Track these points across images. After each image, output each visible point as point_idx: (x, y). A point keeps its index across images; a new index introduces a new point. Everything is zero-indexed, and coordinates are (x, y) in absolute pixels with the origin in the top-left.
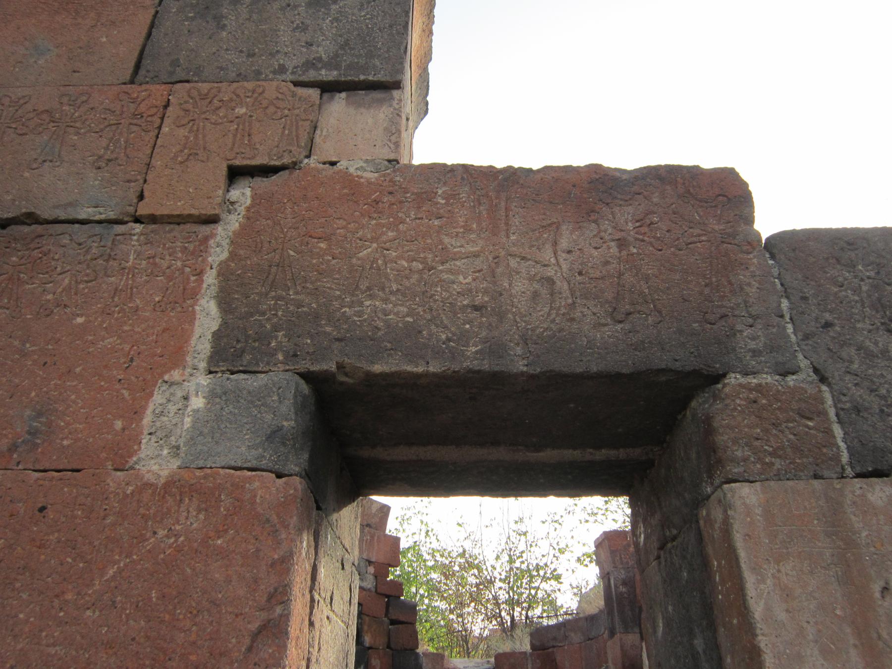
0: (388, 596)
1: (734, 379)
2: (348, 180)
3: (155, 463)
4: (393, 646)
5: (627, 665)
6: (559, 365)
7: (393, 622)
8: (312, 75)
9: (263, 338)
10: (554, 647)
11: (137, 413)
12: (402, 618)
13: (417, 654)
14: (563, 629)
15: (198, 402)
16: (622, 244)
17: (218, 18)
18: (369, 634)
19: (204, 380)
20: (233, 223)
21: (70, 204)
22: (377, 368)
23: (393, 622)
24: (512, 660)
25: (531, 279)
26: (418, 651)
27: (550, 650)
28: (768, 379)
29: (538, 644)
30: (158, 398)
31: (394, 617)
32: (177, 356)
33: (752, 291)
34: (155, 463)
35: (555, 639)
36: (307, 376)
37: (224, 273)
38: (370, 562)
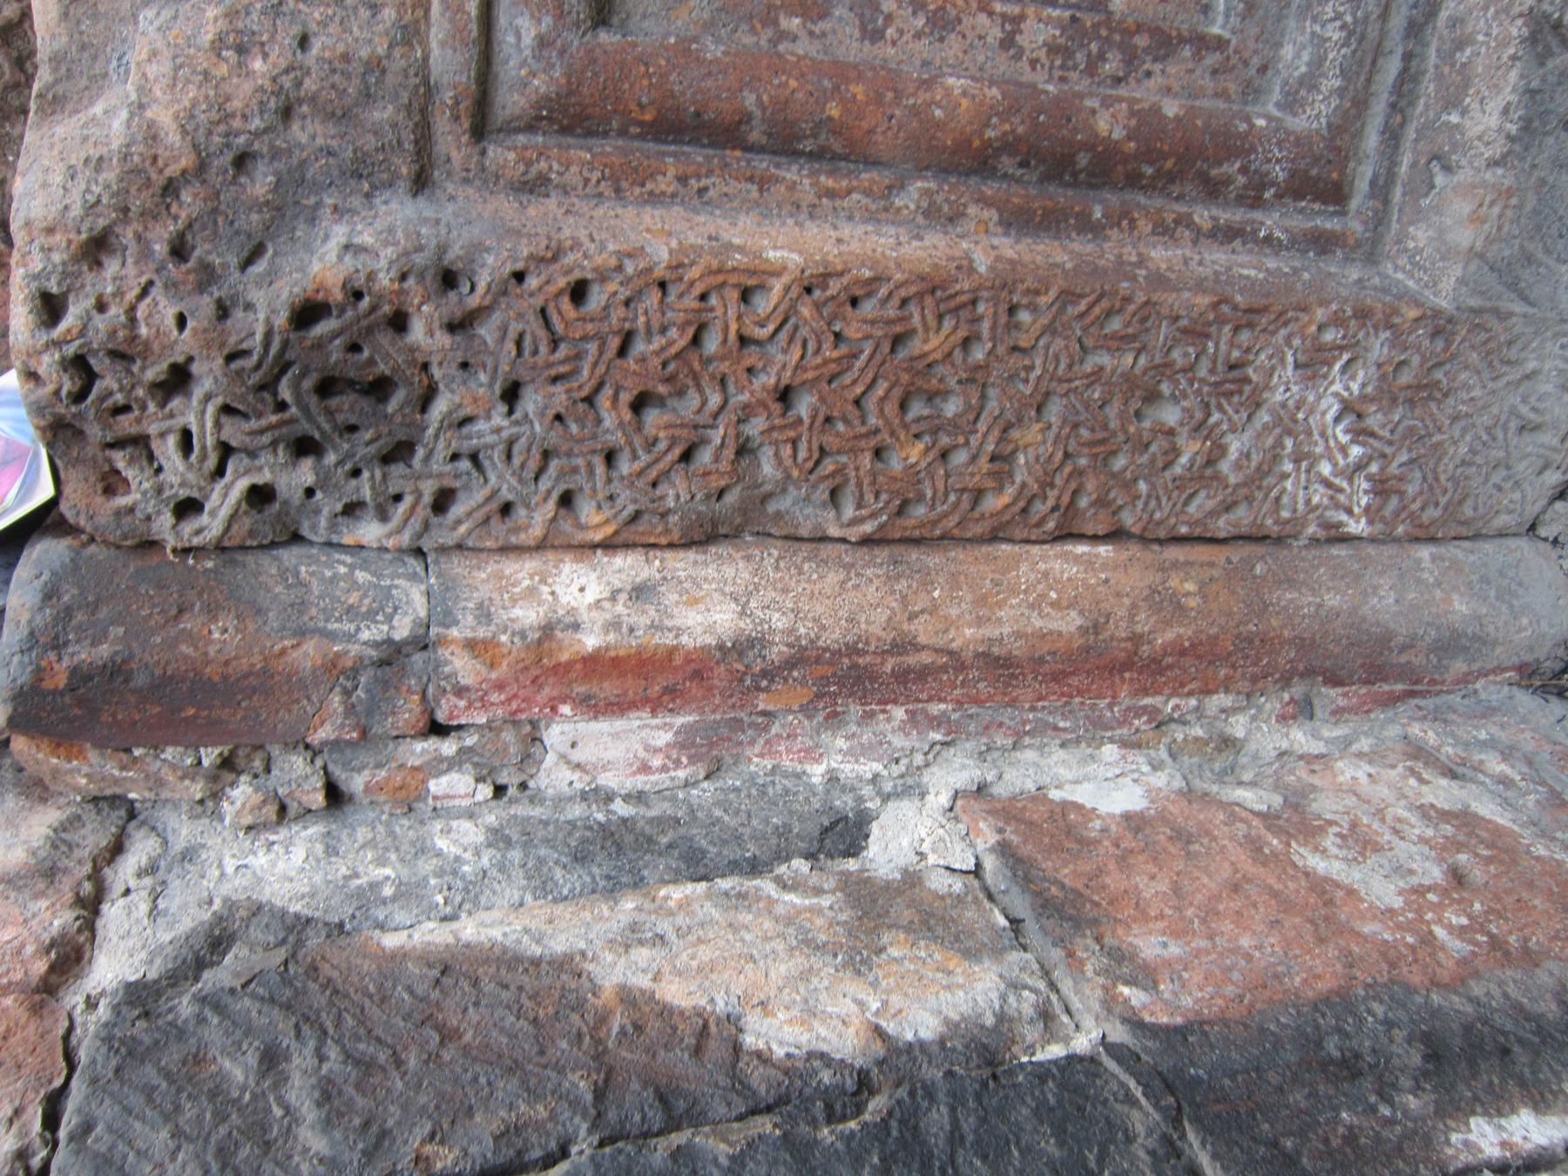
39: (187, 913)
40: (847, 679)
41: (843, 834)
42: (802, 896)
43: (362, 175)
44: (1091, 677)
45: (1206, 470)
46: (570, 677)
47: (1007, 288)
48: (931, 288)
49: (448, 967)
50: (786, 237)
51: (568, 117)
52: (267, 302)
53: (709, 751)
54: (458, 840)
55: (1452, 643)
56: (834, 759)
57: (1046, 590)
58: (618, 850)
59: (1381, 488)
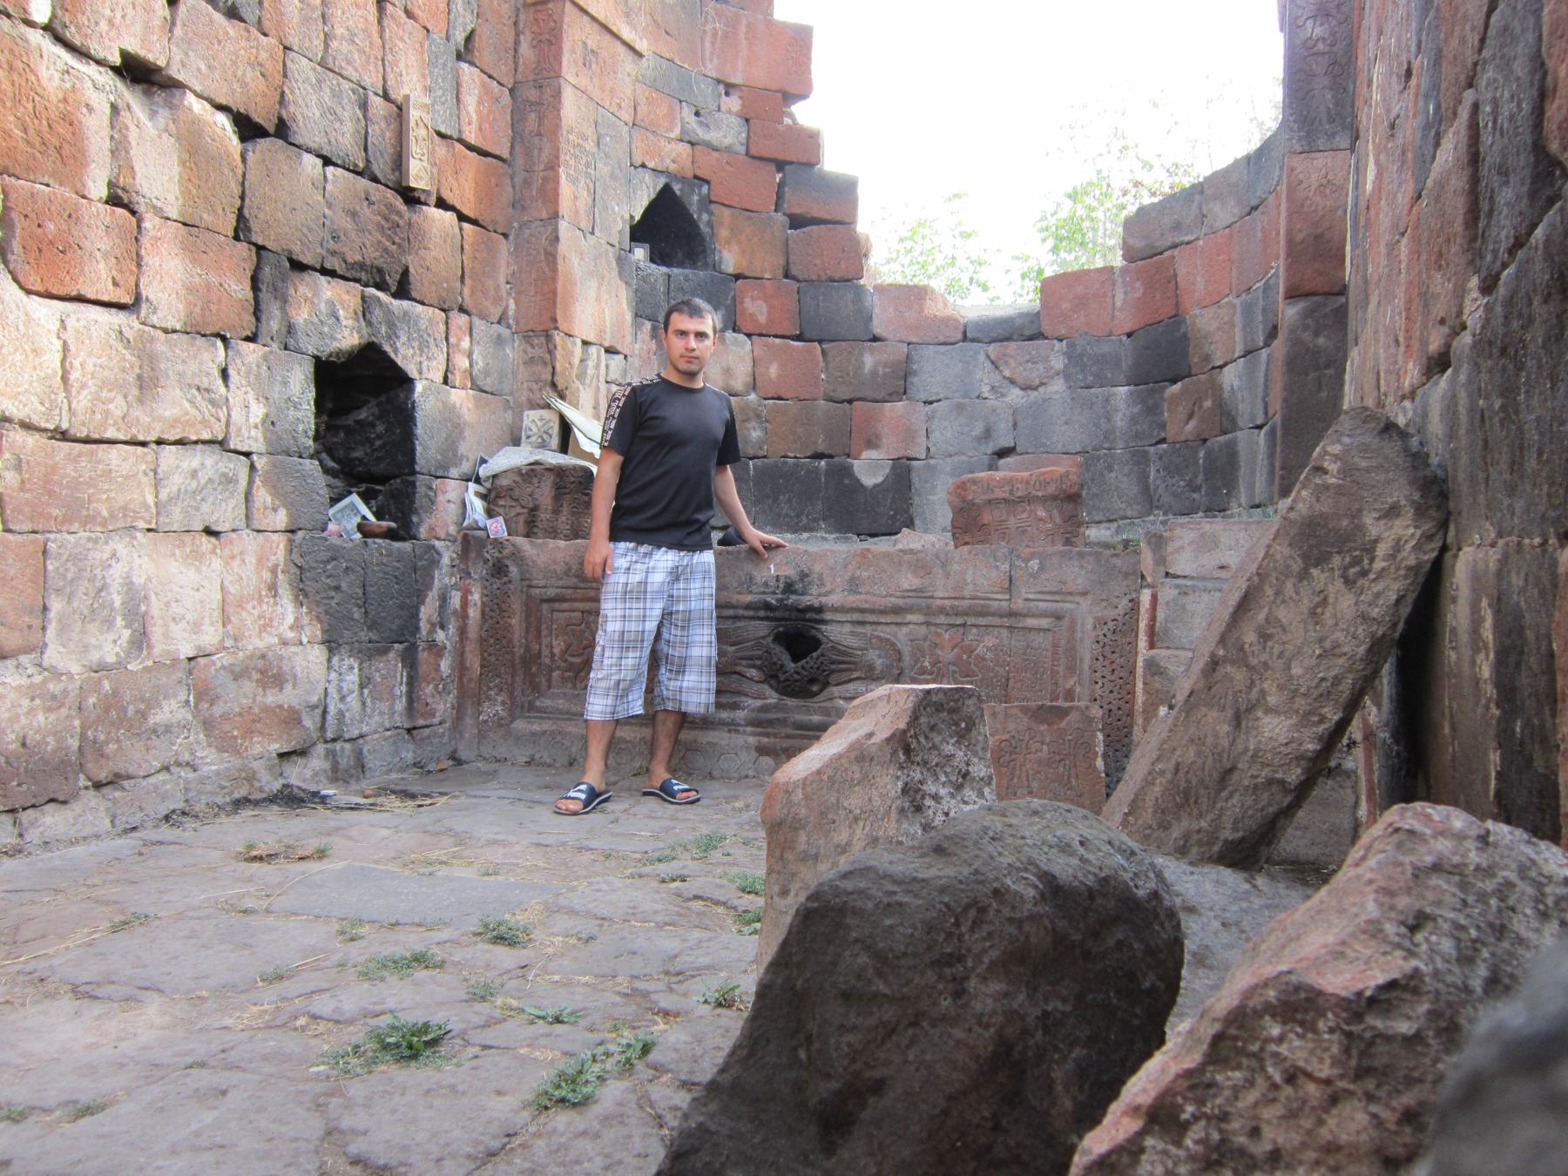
0: (780, 165)
4: (794, 271)
5: (1299, 237)
7: (797, 222)
10: (1174, 246)
12: (815, 213)
13: (859, 292)
14: (1197, 197)
18: (735, 248)
23: (797, 222)
24: (1080, 289)
26: (862, 282)
27: (1166, 254)
29: (1138, 244)
31: (797, 210)
35: (1177, 227)
38: (729, 88)
39: (442, 550)
40: (462, 631)
41: (442, 627)
42: (435, 618)
43: (522, 573)
44: (461, 667)
45: (490, 689)
46: (466, 593)
47: (513, 653)
48: (510, 641)
49: (433, 578)
50: (516, 621)
51: (529, 597)
52: (507, 562)
53: (455, 612)
54: (447, 580)
55: (461, 733)
56: (452, 629)
57: (474, 662)
58: (444, 599)
59: (485, 722)
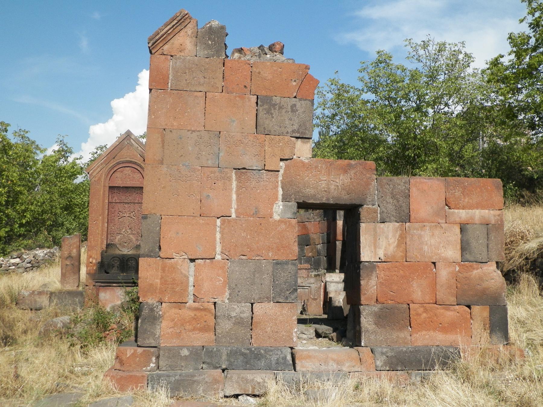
1: (365, 206)
2: (303, 162)
3: (276, 217)
6: (338, 202)
8: (294, 135)
9: (290, 196)
11: (272, 209)
15: (281, 207)
16: (351, 179)
17: (272, 114)
19: (281, 203)
20: (282, 172)
21: (251, 166)
22: (310, 202)
25: (335, 186)
28: (370, 206)
30: (275, 206)
32: (277, 199)
33: (371, 190)
34: (276, 217)
36: (298, 203)
37: (282, 183)
